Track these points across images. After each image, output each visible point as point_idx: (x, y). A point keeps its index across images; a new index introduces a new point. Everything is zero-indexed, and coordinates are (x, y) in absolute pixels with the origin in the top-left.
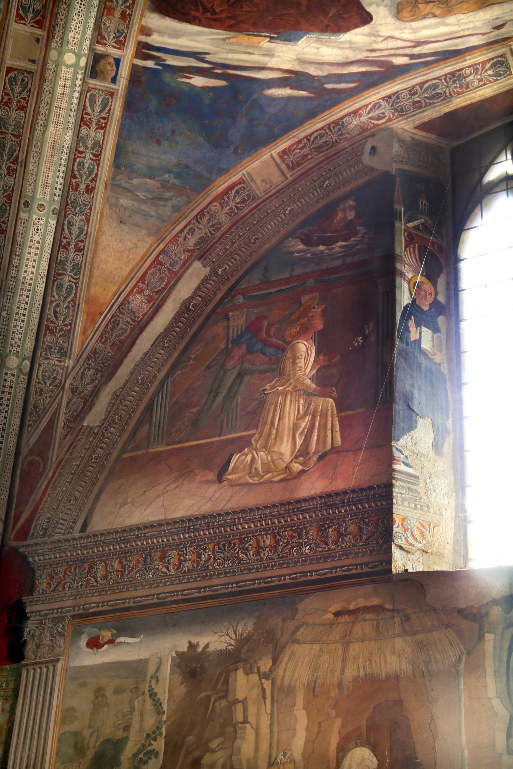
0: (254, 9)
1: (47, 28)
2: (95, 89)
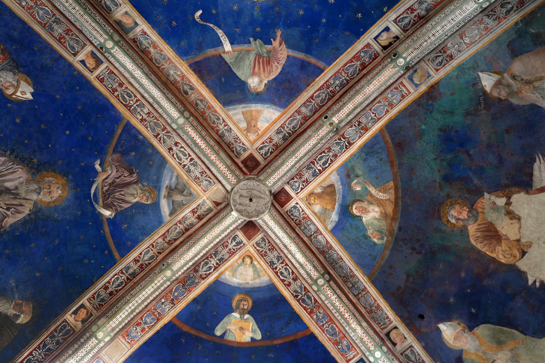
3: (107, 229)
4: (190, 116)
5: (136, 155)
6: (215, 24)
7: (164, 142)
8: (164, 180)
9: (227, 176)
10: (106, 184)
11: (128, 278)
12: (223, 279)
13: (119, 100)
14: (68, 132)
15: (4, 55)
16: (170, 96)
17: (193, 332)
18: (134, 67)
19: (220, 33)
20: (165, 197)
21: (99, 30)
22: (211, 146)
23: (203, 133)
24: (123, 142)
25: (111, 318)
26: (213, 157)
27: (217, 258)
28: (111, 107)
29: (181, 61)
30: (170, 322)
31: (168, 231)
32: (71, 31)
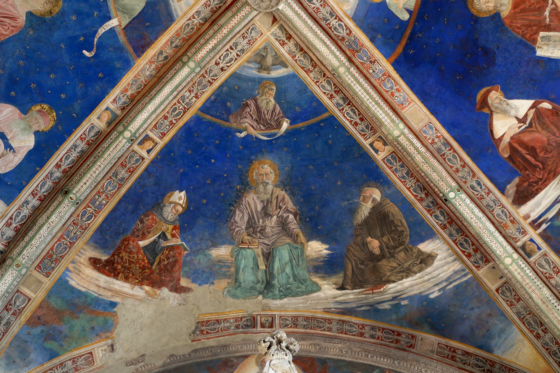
0: (554, 159)
1: (492, 260)
2: (537, 260)
3: (300, 125)
4: (186, 55)
5: (230, 102)
6: (94, 37)
7: (216, 76)
8: (253, 75)
9: (243, 16)
10: (258, 127)
11: (348, 104)
12: (351, 12)
13: (180, 119)
14: (213, 161)
15: (150, 215)
16: (169, 76)
17: (404, 42)
18: (145, 111)
19: (101, 31)
20: (268, 73)
21: (115, 144)
22: (214, 33)
23: (202, 41)
24: (218, 114)
25: (381, 124)
26: (225, 31)
27: (330, 18)
28: (187, 126)
29: (136, 65)
30: (393, 65)
31: (302, 68)
32: (122, 163)
